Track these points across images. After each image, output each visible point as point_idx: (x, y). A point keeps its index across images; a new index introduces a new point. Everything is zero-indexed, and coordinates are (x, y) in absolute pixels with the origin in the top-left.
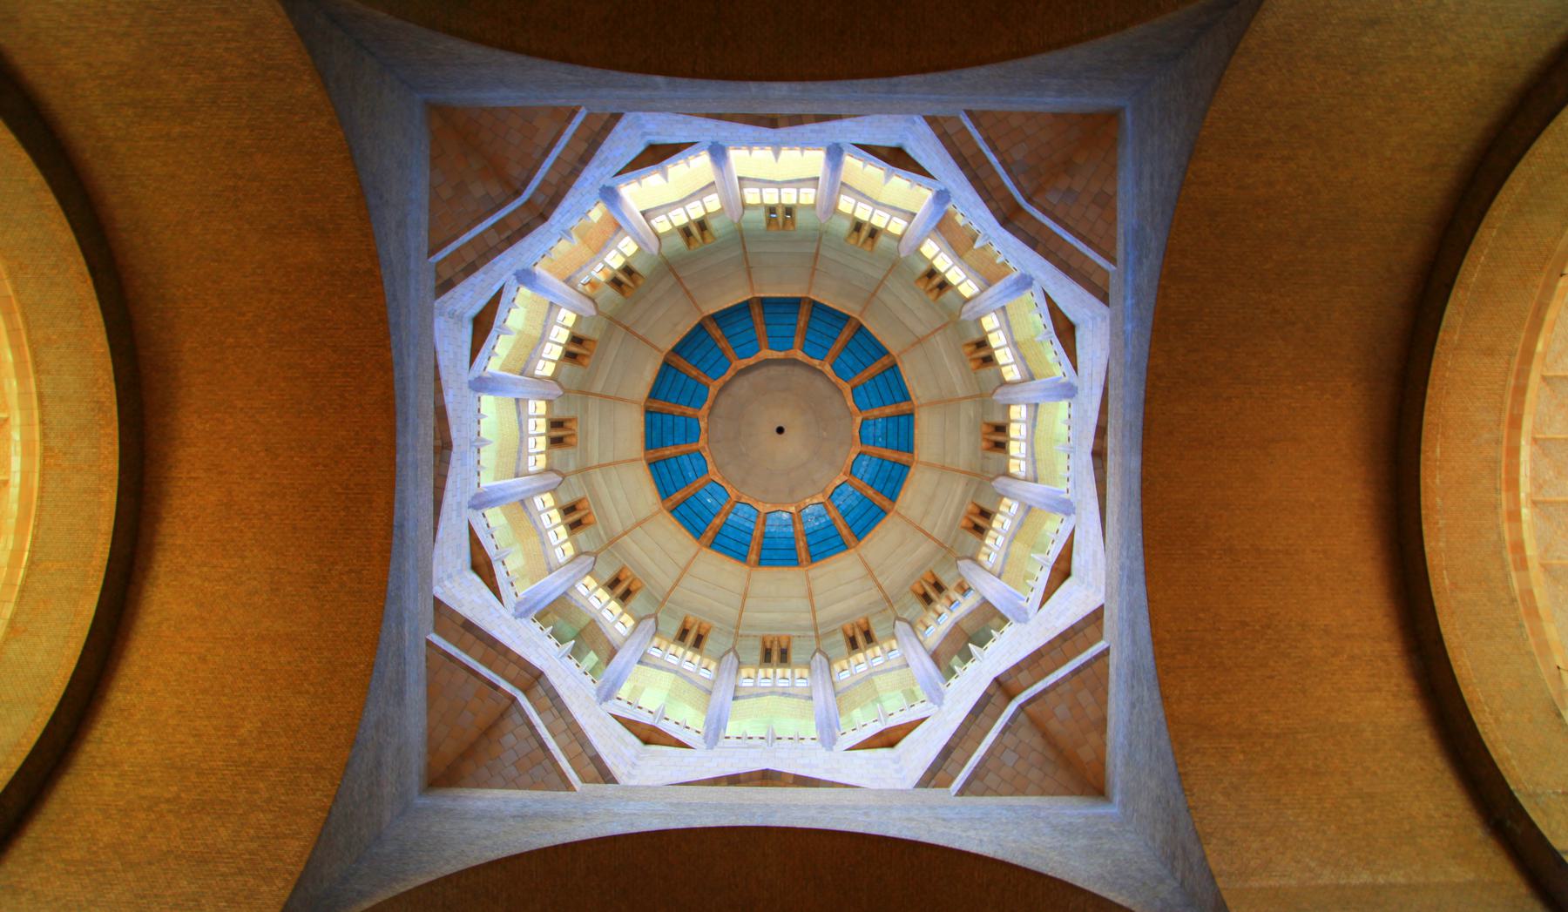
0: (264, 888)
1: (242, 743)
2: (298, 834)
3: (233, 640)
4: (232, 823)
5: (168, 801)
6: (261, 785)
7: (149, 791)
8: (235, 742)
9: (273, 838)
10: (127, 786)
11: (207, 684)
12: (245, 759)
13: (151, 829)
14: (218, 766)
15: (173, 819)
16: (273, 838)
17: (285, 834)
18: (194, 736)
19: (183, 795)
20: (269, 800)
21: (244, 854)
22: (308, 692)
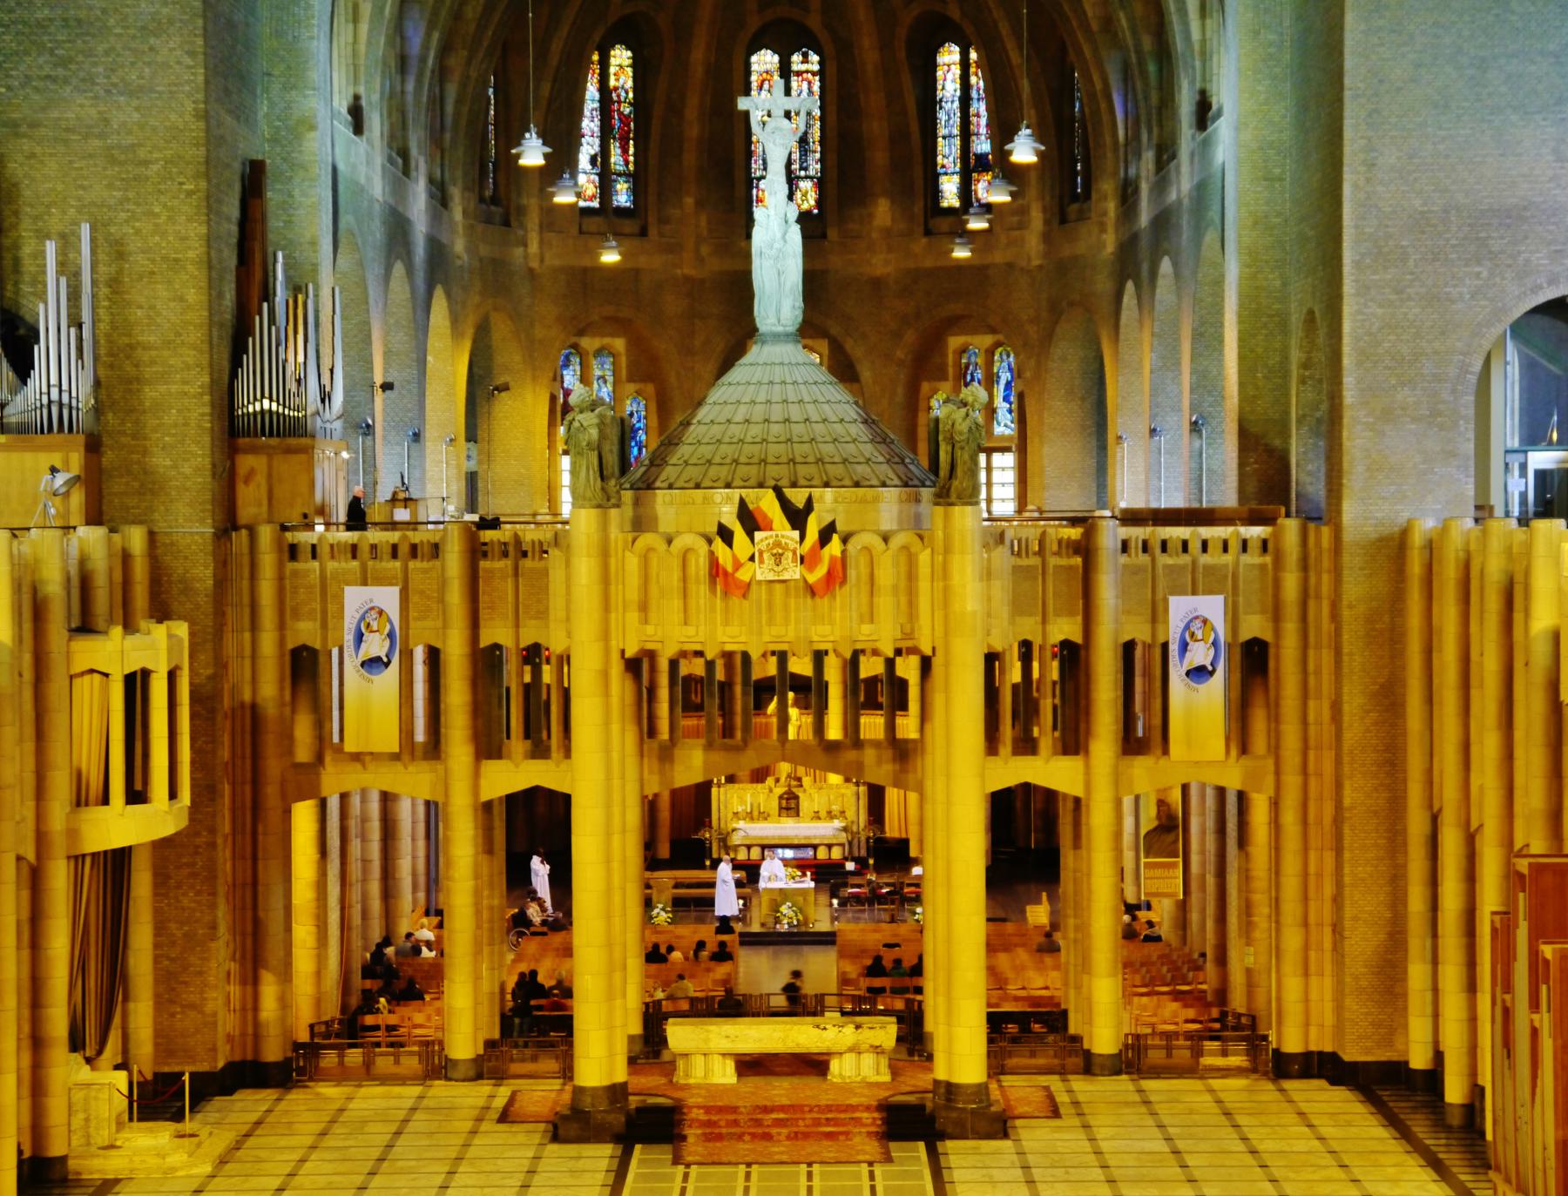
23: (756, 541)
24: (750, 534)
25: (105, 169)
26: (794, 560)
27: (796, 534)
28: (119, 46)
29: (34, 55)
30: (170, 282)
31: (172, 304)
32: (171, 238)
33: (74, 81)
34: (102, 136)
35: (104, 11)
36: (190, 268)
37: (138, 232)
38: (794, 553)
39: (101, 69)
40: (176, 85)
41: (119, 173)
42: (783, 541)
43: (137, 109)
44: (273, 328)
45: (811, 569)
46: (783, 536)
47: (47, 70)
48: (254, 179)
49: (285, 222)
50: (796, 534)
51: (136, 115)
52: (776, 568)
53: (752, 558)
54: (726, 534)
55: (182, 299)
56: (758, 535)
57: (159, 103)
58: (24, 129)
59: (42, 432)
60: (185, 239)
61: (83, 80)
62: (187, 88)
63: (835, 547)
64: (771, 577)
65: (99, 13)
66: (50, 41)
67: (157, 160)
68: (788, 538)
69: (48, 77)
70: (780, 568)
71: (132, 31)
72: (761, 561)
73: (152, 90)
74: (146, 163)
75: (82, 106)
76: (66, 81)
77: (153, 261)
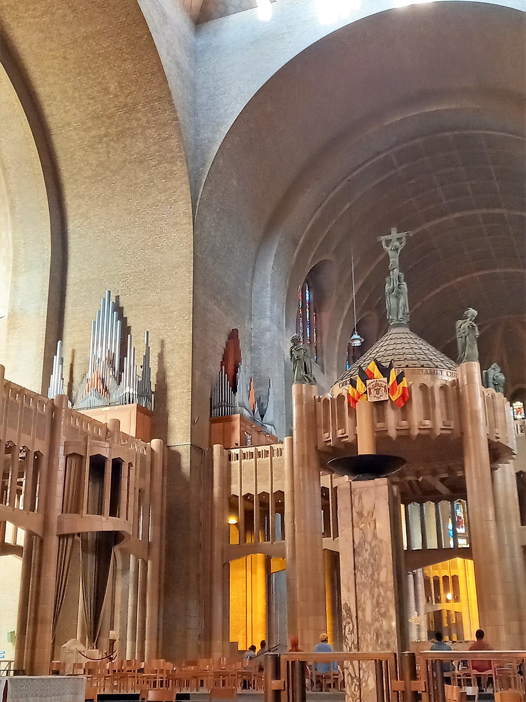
0: (174, 168)
1: (116, 96)
2: (171, 136)
3: (72, 43)
4: (140, 138)
5: (106, 135)
6: (139, 115)
7: (93, 133)
8: (112, 96)
9: (162, 141)
10: (82, 134)
11: (78, 71)
12: (123, 104)
13: (109, 152)
14: (113, 111)
15: (113, 144)
16: (162, 141)
17: (166, 137)
18: (92, 99)
19: (109, 131)
20: (148, 122)
21: (156, 153)
22: (128, 59)
23: (367, 385)
24: (364, 381)
25: (159, 316)
26: (385, 391)
27: (386, 378)
28: (166, 274)
29: (138, 282)
30: (178, 352)
31: (179, 360)
32: (180, 337)
33: (151, 288)
34: (159, 305)
35: (161, 264)
36: (186, 346)
37: (169, 336)
38: (385, 387)
39: (159, 283)
40: (183, 283)
41: (163, 317)
42: (380, 383)
43: (170, 294)
44: (226, 375)
45: (393, 394)
46: (379, 381)
47: (142, 286)
48: (233, 335)
49: (258, 364)
50: (385, 379)
51: (170, 296)
52: (377, 396)
53: (366, 392)
54: (353, 384)
55: (182, 358)
56: (368, 382)
57: (178, 291)
58: (134, 307)
59: (123, 404)
60: (185, 336)
61: (154, 287)
62: (187, 284)
63: (404, 383)
64: (375, 400)
65: (160, 264)
66: (144, 277)
67: (176, 310)
68: (382, 381)
69: (143, 288)
70: (379, 395)
71: (170, 268)
72: (370, 393)
73: (176, 287)
74: (172, 312)
75: (153, 296)
76: (148, 289)
77: (173, 346)
